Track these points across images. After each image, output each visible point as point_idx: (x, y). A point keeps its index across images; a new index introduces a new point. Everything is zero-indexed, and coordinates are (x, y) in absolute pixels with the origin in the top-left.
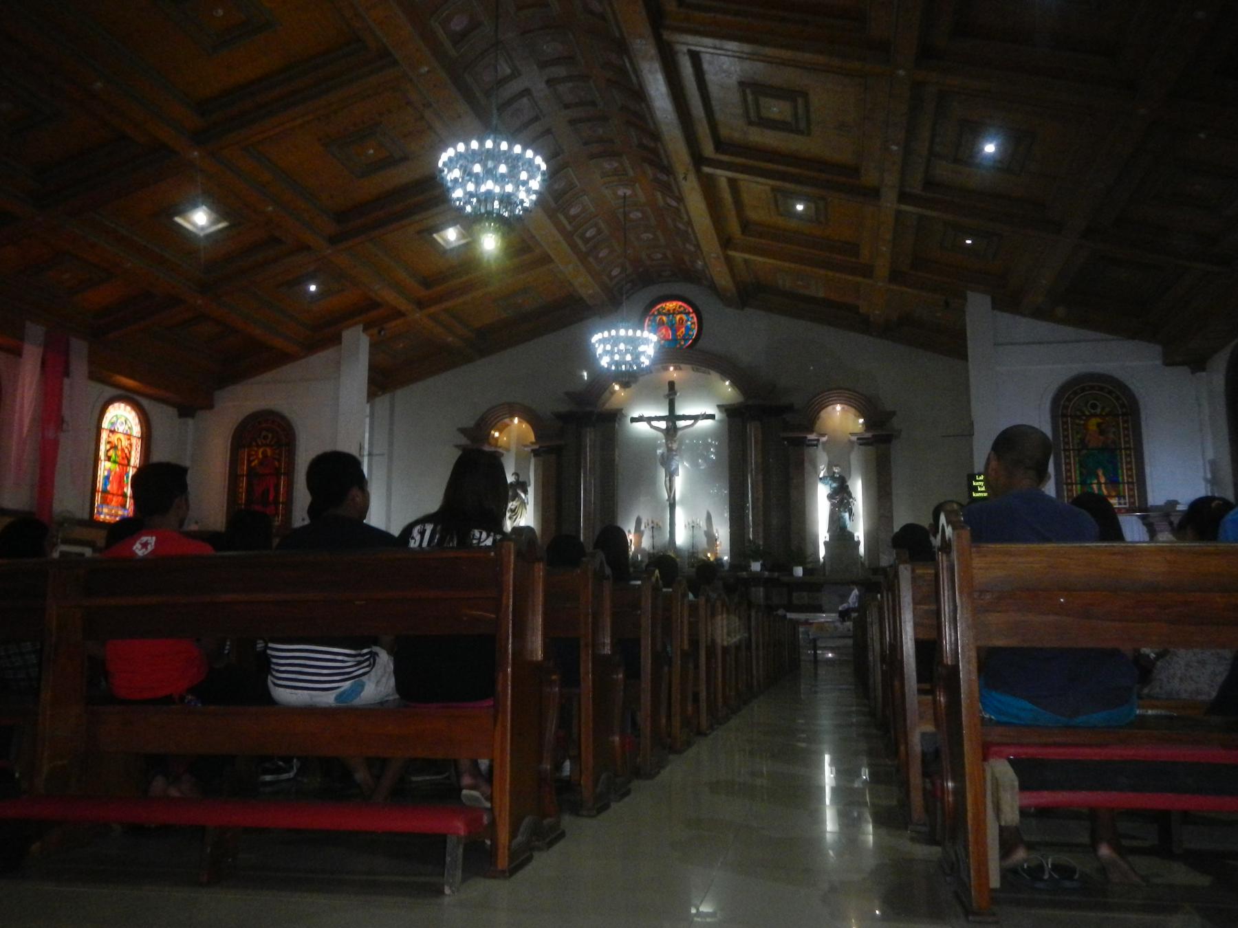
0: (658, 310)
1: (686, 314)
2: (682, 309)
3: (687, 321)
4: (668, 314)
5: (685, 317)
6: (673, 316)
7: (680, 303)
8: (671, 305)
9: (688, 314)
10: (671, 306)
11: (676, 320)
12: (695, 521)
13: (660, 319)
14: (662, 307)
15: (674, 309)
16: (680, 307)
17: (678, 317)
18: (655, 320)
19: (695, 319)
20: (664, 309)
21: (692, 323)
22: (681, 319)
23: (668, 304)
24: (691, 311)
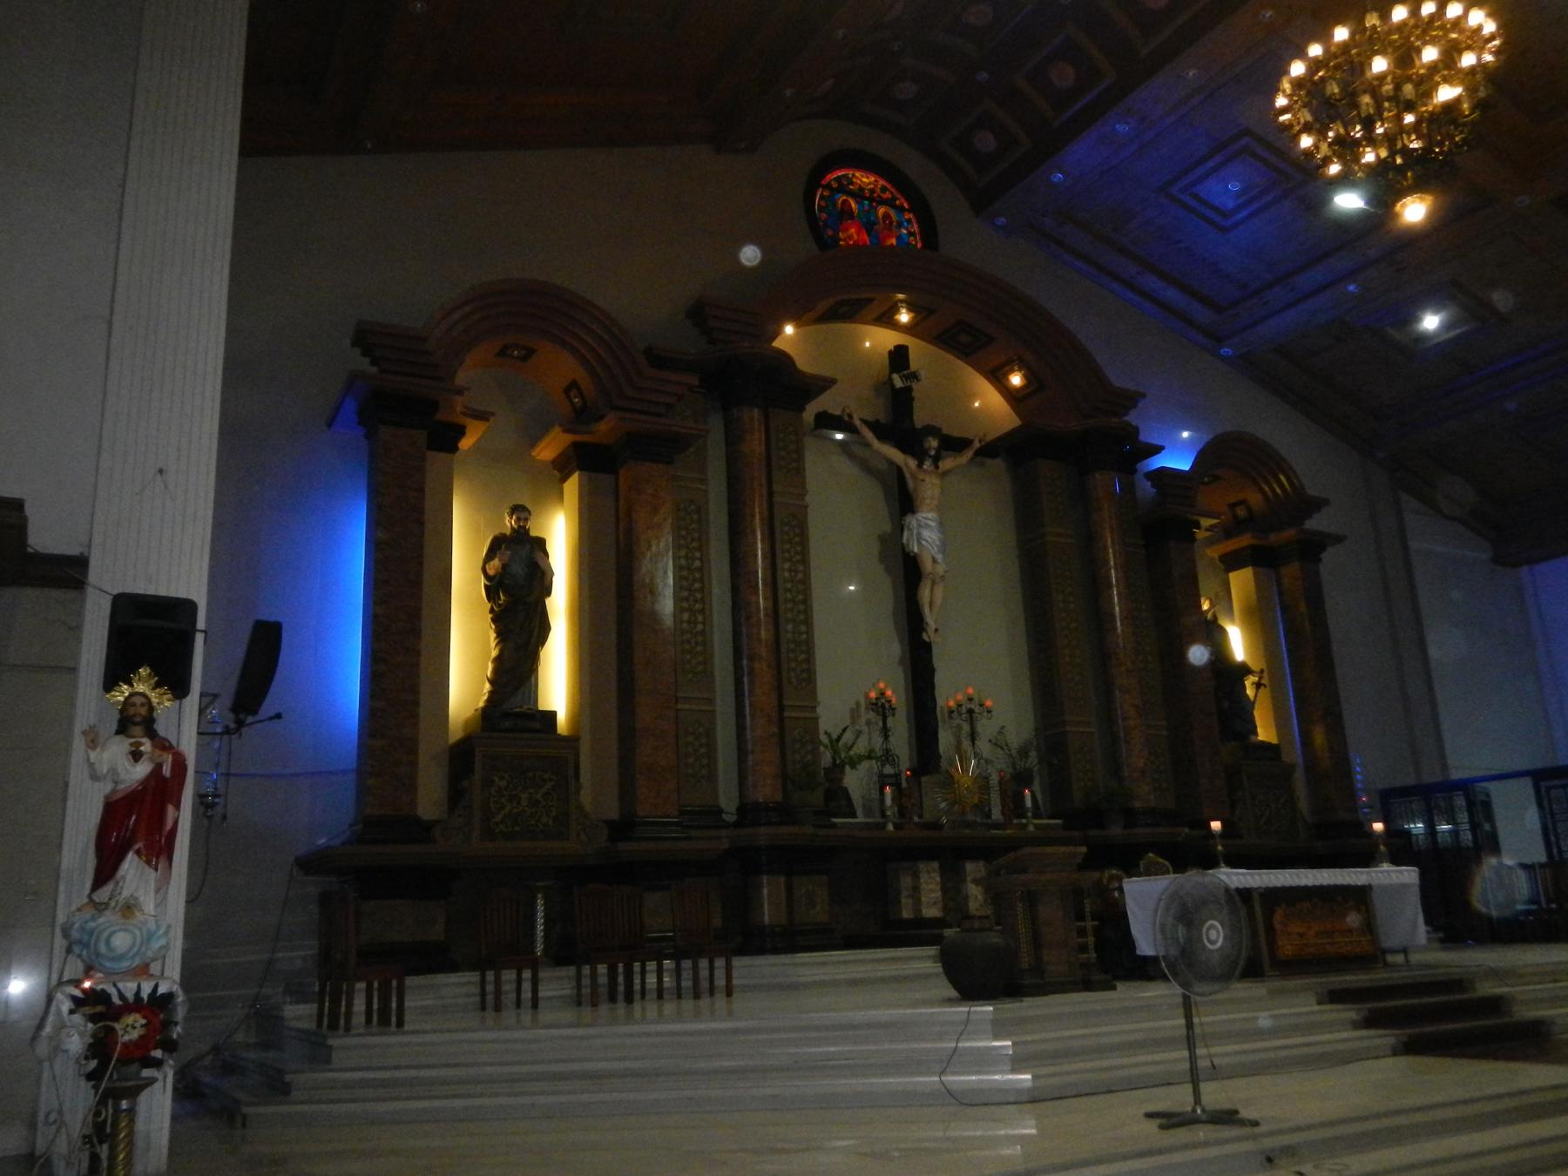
0: (838, 179)
1: (894, 207)
2: (887, 195)
3: (900, 225)
4: (859, 195)
5: (892, 213)
6: (871, 206)
7: (882, 182)
8: (865, 179)
9: (900, 209)
10: (865, 180)
11: (877, 217)
12: (976, 699)
13: (844, 201)
14: (845, 176)
15: (872, 191)
16: (884, 189)
17: (882, 210)
18: (835, 204)
19: (915, 228)
20: (852, 183)
21: (910, 234)
22: (886, 216)
23: (857, 174)
24: (906, 205)
